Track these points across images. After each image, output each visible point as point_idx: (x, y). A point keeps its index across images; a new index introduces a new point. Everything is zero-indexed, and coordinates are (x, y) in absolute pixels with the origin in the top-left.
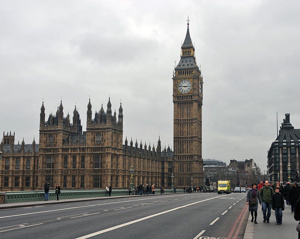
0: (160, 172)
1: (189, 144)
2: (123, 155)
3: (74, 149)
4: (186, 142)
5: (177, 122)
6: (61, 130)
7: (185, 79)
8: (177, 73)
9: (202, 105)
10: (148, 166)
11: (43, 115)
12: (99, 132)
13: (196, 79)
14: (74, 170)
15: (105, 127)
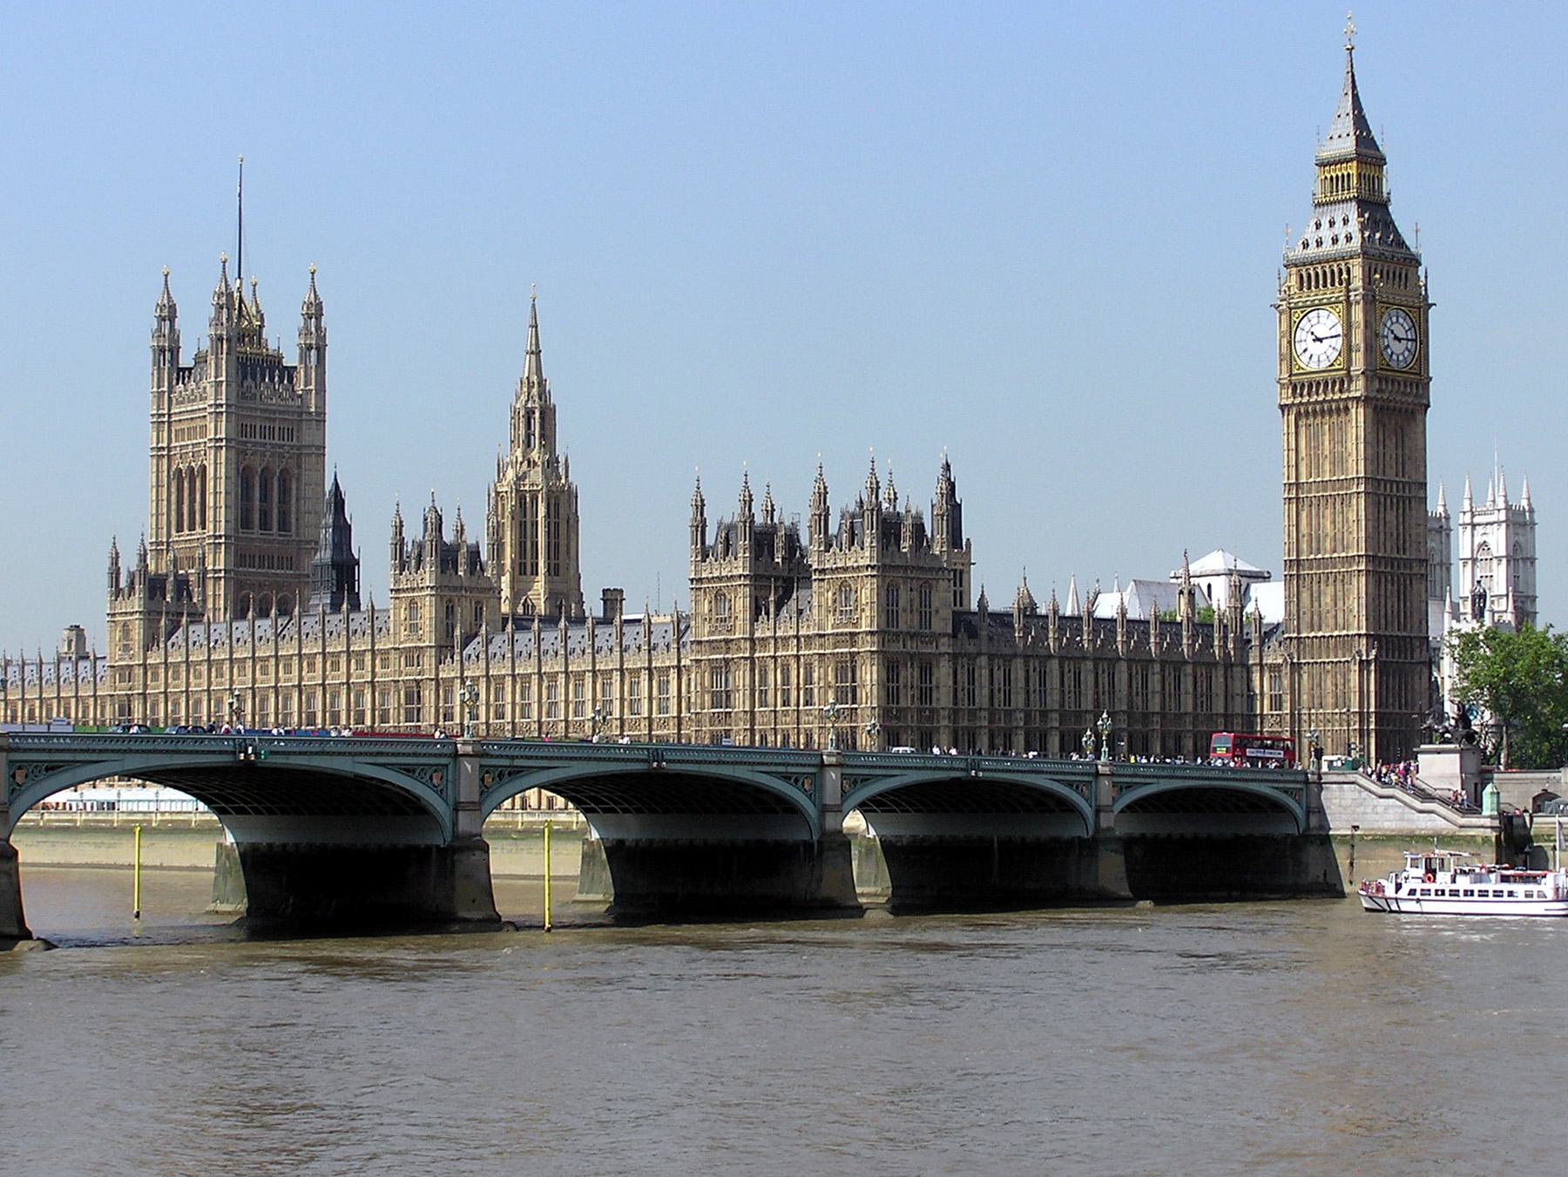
0: (1238, 710)
1: (1339, 586)
2: (954, 657)
3: (786, 639)
4: (1331, 580)
5: (1297, 494)
6: (745, 576)
7: (1317, 306)
8: (1294, 280)
9: (1428, 406)
10: (1150, 689)
11: (700, 527)
12: (844, 582)
13: (1358, 303)
14: (785, 713)
15: (862, 563)
